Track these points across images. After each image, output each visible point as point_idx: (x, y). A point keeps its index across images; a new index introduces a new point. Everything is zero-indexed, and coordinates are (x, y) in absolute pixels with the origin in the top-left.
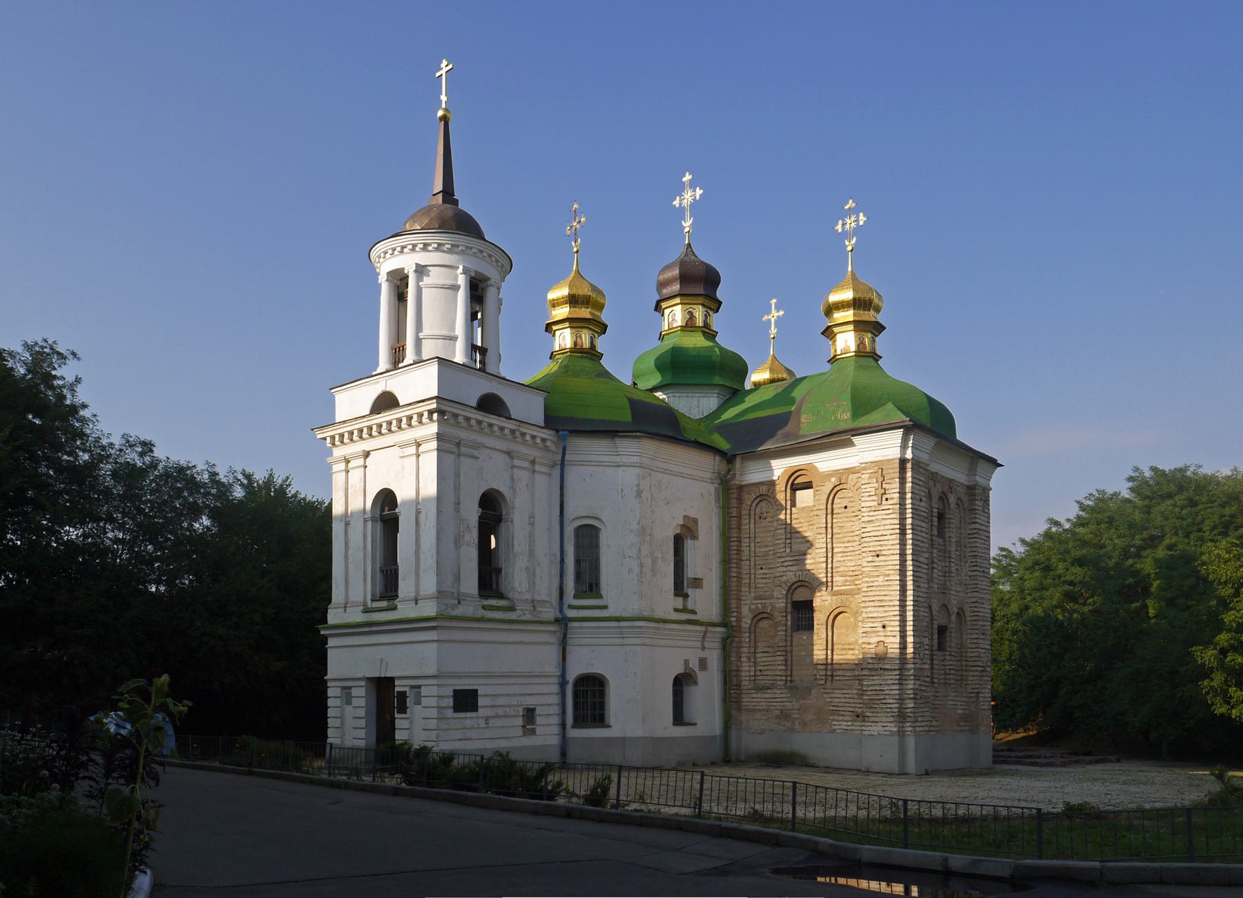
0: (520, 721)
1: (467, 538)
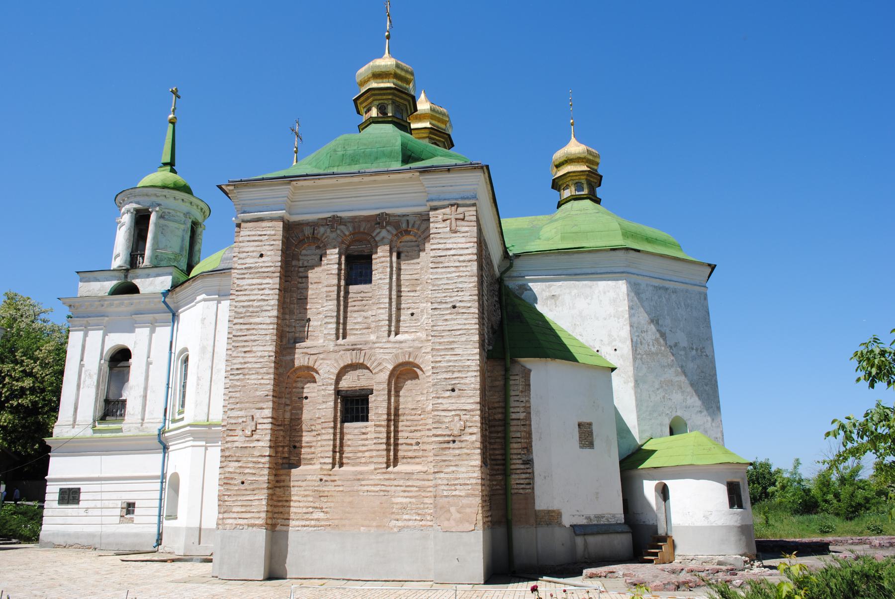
0: (118, 512)
1: (88, 381)
